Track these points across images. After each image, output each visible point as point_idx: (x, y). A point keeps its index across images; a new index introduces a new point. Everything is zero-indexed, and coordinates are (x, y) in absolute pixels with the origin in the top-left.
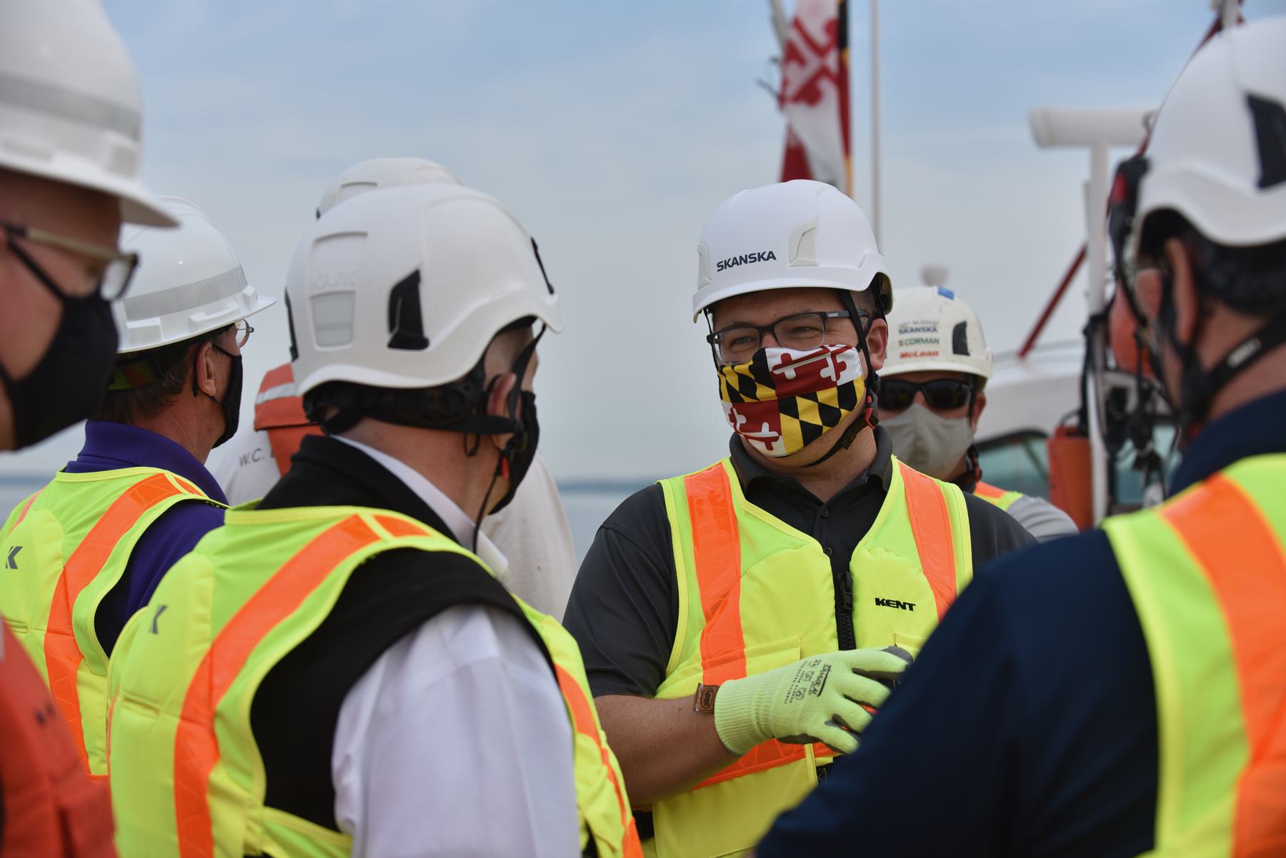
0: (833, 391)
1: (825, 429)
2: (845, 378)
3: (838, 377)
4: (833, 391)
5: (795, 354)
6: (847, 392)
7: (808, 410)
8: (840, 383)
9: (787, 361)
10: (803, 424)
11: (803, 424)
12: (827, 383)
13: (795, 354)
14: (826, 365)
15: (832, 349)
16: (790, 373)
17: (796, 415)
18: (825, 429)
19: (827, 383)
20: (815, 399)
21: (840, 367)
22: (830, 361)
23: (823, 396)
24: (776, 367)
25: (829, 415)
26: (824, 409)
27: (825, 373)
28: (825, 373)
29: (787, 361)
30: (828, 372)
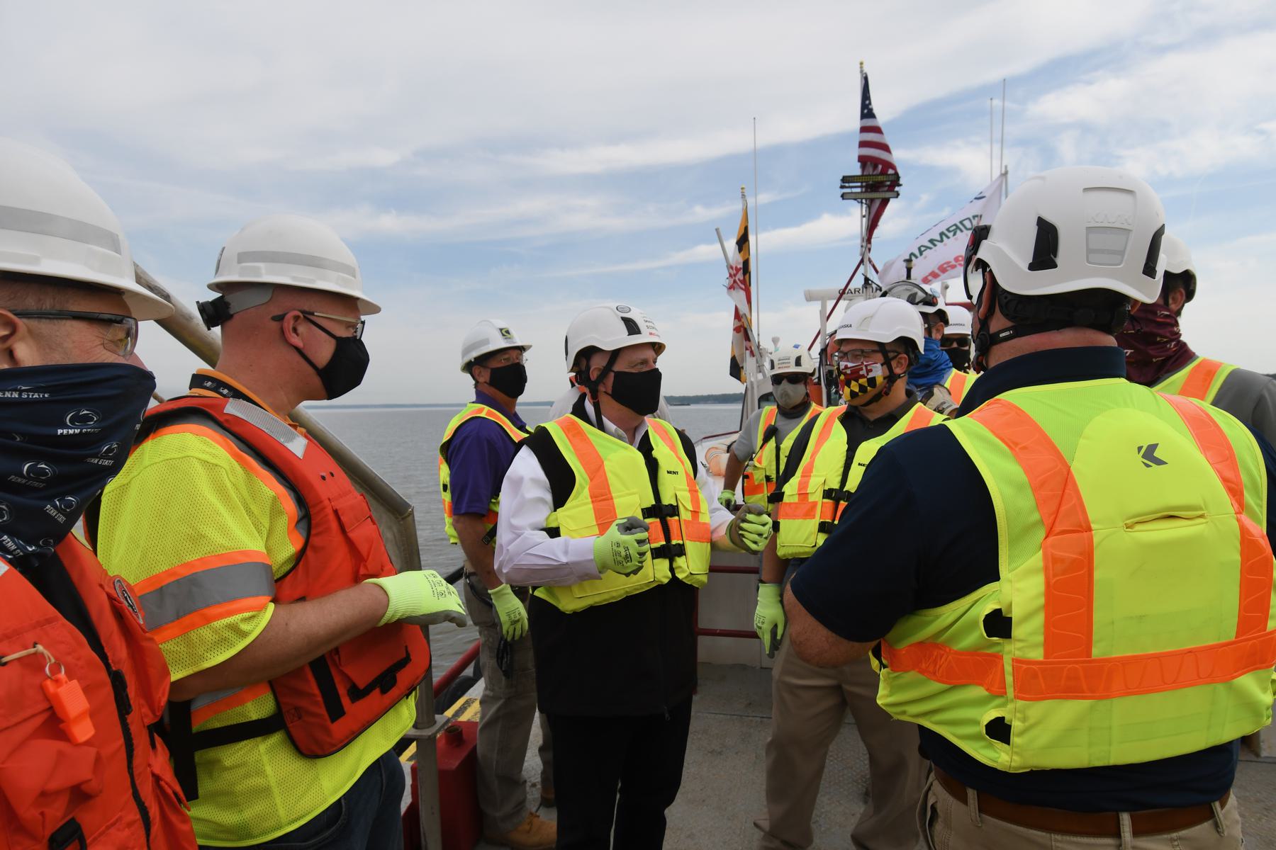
0: (865, 379)
1: (860, 394)
2: (871, 375)
3: (868, 375)
4: (865, 379)
5: (850, 365)
6: (872, 382)
7: (855, 386)
8: (868, 377)
9: (846, 367)
10: (851, 390)
11: (851, 390)
12: (863, 376)
13: (850, 365)
14: (862, 369)
15: (865, 363)
16: (848, 371)
17: (850, 387)
18: (860, 394)
19: (863, 376)
20: (857, 381)
21: (869, 371)
22: (864, 368)
23: (861, 381)
24: (843, 370)
25: (862, 388)
26: (861, 387)
27: (861, 373)
28: (861, 373)
29: (846, 367)
30: (863, 372)
